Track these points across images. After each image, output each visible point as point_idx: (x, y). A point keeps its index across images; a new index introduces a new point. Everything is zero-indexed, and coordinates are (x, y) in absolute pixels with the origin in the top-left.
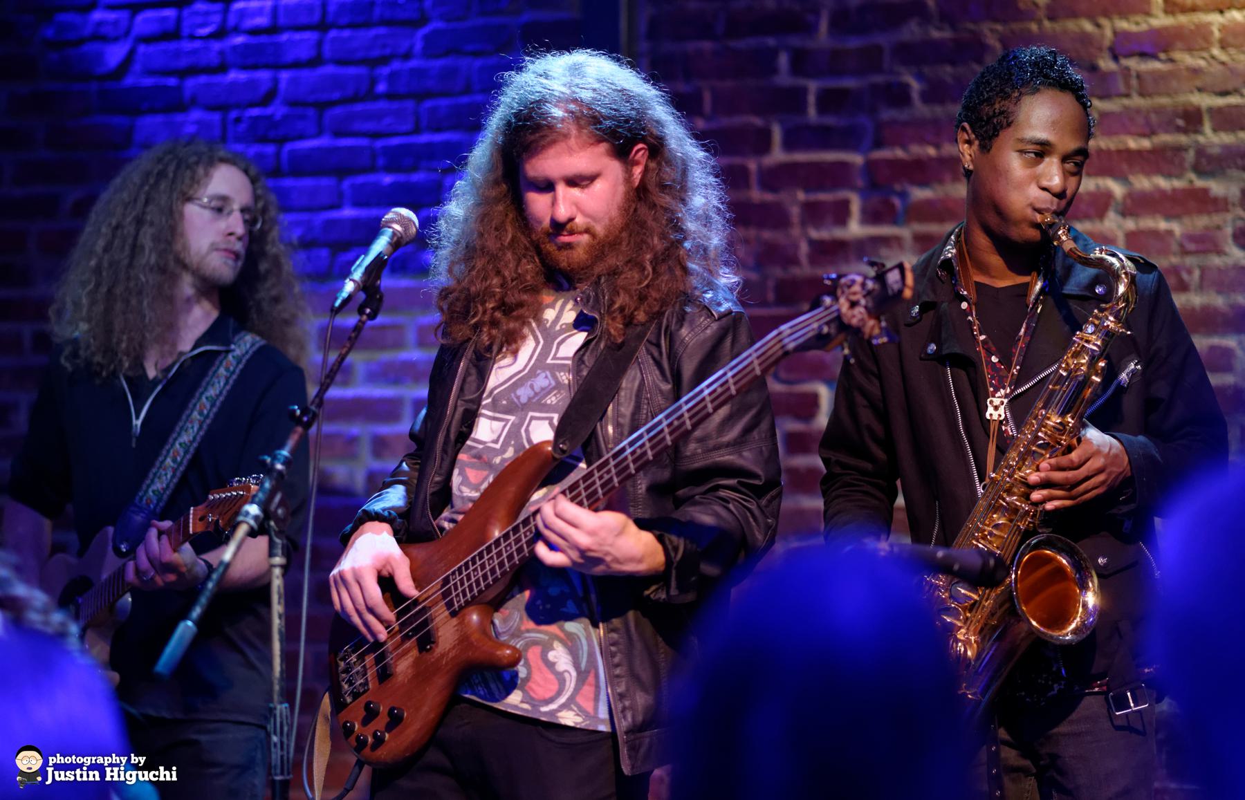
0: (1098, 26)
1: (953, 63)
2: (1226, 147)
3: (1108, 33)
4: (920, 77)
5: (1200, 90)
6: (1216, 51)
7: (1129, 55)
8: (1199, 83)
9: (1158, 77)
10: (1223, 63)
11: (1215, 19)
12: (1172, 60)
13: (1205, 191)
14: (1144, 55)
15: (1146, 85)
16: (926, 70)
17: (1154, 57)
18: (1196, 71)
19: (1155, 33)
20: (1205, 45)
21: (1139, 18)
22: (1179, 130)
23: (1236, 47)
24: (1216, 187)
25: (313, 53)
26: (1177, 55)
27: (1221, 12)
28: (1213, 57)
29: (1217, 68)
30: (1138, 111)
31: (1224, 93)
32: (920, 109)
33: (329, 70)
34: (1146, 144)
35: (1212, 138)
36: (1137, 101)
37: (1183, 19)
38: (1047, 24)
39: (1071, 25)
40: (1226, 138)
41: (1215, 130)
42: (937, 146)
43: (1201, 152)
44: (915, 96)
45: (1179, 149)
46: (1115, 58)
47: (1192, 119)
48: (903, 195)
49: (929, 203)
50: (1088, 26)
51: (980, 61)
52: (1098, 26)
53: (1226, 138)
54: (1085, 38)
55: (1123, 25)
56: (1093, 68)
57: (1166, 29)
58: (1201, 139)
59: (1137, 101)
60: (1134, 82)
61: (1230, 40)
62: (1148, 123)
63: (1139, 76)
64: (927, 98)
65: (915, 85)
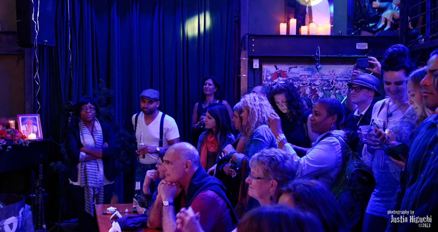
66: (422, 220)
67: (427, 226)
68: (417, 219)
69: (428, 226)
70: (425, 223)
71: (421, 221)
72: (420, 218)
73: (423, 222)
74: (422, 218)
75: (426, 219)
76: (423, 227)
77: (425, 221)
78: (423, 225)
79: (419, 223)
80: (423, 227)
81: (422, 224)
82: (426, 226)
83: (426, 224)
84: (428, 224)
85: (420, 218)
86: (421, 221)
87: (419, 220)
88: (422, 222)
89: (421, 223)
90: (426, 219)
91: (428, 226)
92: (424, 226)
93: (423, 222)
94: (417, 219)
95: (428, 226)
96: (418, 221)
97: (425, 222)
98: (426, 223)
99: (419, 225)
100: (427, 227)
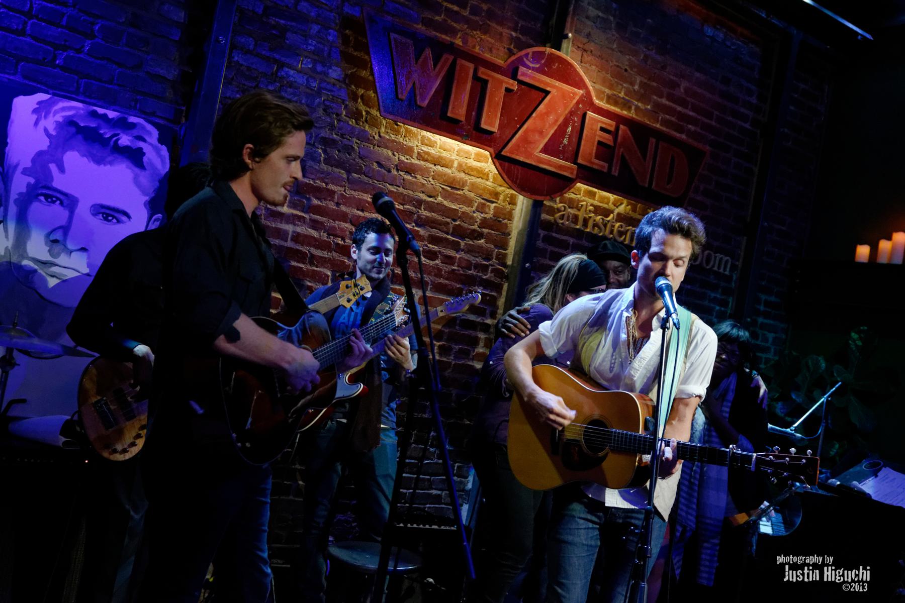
0: (394, 155)
1: (339, 151)
2: (427, 217)
3: (396, 158)
4: (325, 151)
5: (423, 192)
6: (431, 179)
7: (401, 171)
8: (423, 189)
9: (415, 183)
10: (432, 184)
11: (432, 166)
12: (416, 177)
13: (418, 231)
14: (408, 173)
15: (404, 184)
16: (329, 150)
17: (410, 174)
18: (423, 184)
19: (412, 164)
20: (428, 176)
21: (408, 157)
22: (414, 205)
23: (438, 180)
24: (422, 231)
25: (20, 27)
26: (418, 177)
27: (435, 165)
28: (430, 182)
29: (430, 186)
30: (402, 193)
31: (430, 197)
32: (324, 167)
33: (28, 39)
34: (401, 207)
35: (425, 213)
36: (401, 190)
37: (422, 163)
38: (376, 146)
39: (385, 150)
40: (428, 214)
41: (425, 210)
42: (327, 184)
43: (419, 217)
44: (322, 159)
45: (412, 213)
46: (398, 170)
47: (419, 203)
48: (309, 199)
49: (319, 206)
50: (390, 153)
51: (349, 155)
52: (394, 155)
53: (428, 214)
54: (389, 159)
55: (403, 158)
56: (389, 171)
57: (416, 164)
58: (420, 211)
59: (401, 190)
60: (402, 181)
61: (436, 176)
62: (404, 200)
63: (404, 180)
64: (327, 162)
65: (322, 155)
66: (850, 575)
67: (860, 589)
68: (839, 573)
69: (863, 589)
70: (855, 582)
71: (848, 578)
72: (846, 572)
73: (853, 581)
74: (850, 572)
75: (857, 573)
76: (852, 590)
77: (855, 577)
78: (851, 587)
79: (844, 582)
80: (852, 590)
81: (850, 583)
82: (857, 588)
83: (859, 585)
84: (863, 584)
85: (846, 572)
86: (848, 578)
87: (843, 575)
88: (850, 580)
89: (847, 582)
90: (857, 573)
91: (863, 588)
92: (854, 588)
93: (853, 581)
94: (839, 573)
95: (863, 588)
96: (842, 578)
97: (856, 579)
98: (858, 581)
99: (844, 587)
100: (861, 590)
